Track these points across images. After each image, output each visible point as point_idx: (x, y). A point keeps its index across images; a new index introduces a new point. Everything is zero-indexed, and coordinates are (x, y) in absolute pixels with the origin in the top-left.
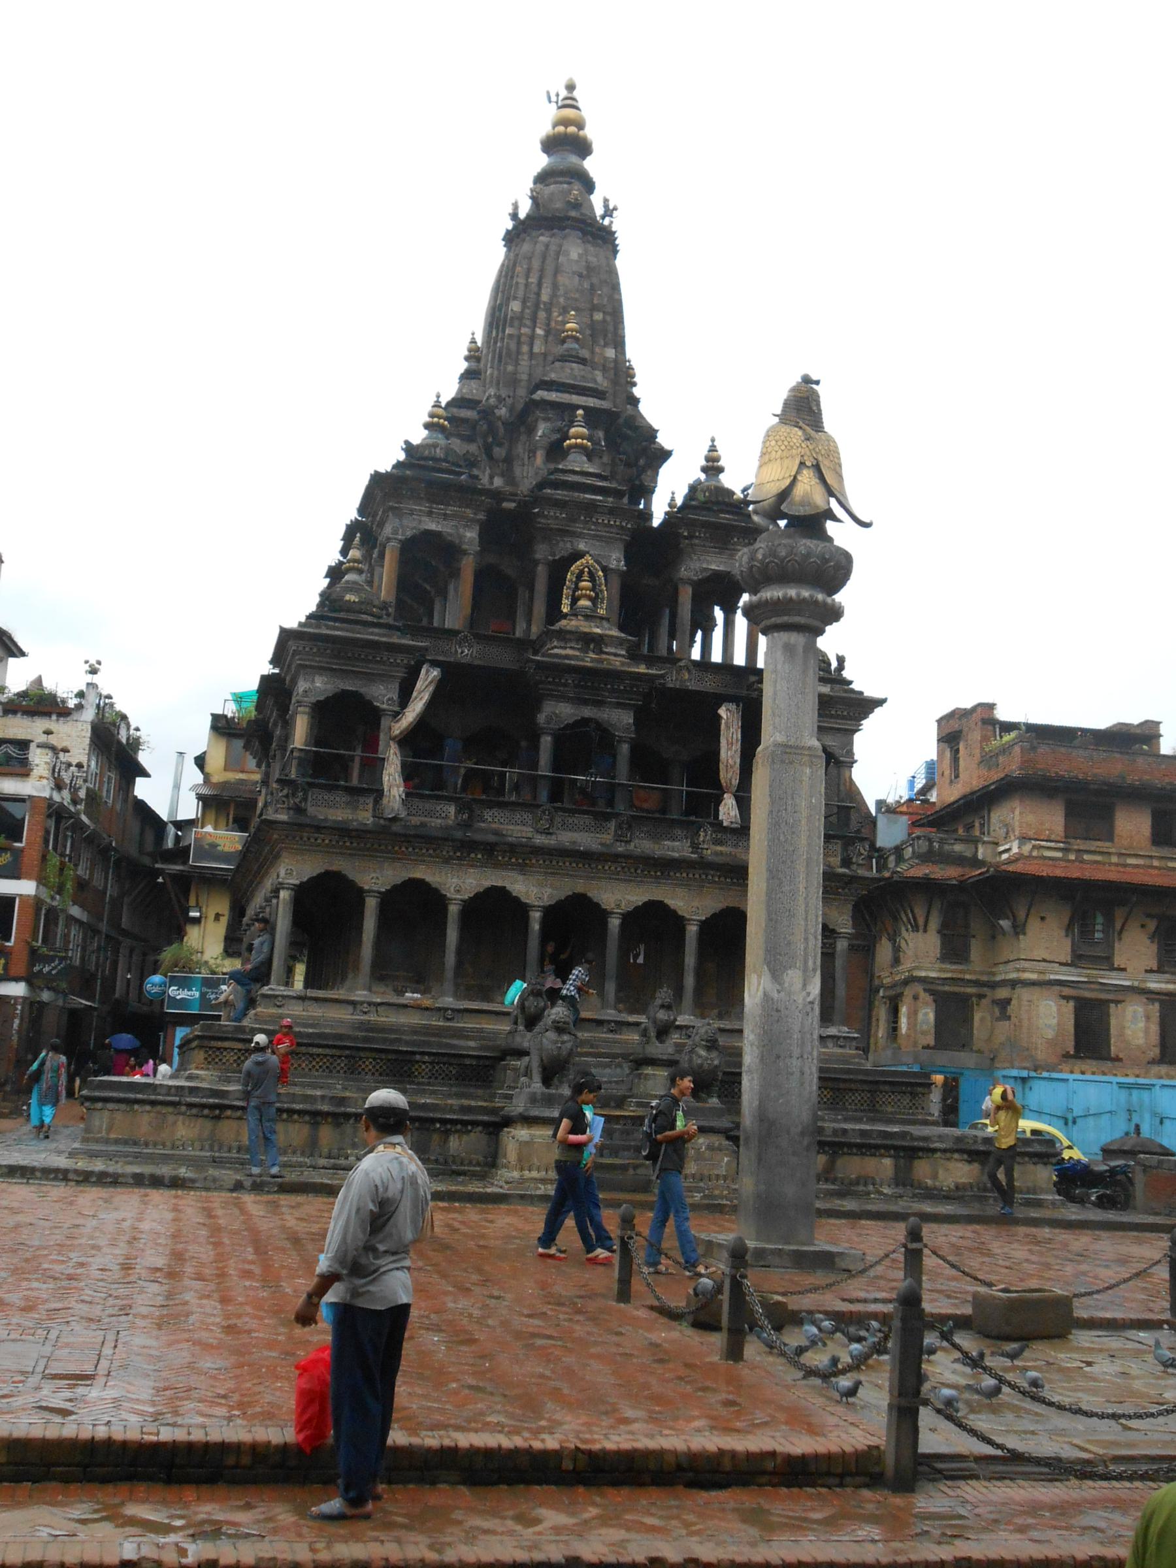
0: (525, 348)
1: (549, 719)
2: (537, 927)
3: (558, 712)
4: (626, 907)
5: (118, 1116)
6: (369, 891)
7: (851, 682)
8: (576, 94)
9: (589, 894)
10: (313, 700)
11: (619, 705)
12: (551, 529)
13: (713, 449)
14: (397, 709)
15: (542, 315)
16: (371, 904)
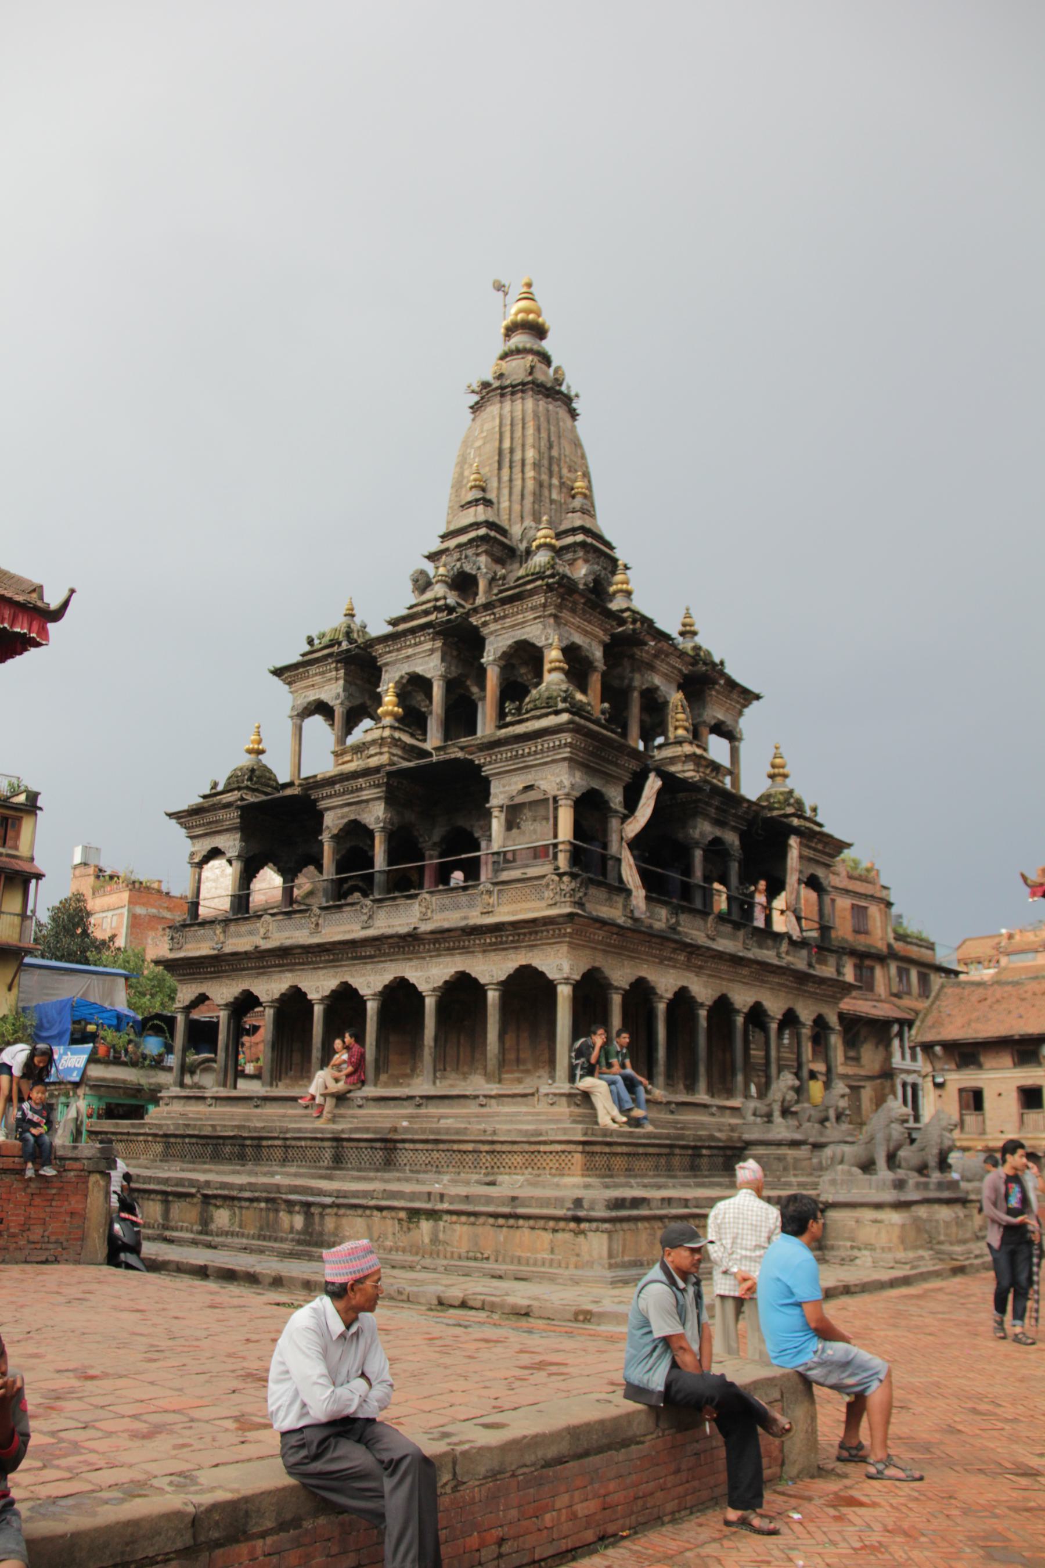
0: (546, 492)
1: (702, 834)
2: (703, 1023)
3: (704, 829)
4: (745, 1010)
5: (628, 1236)
6: (617, 988)
7: (820, 825)
8: (532, 290)
9: (730, 995)
10: (577, 794)
11: (734, 829)
12: (642, 662)
13: (688, 615)
14: (626, 812)
15: (555, 468)
16: (617, 999)
